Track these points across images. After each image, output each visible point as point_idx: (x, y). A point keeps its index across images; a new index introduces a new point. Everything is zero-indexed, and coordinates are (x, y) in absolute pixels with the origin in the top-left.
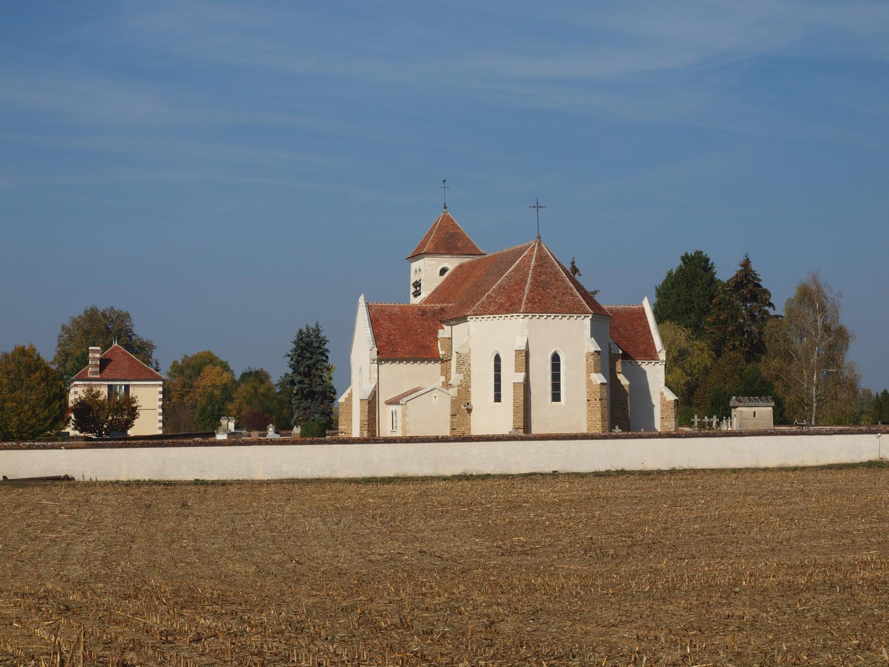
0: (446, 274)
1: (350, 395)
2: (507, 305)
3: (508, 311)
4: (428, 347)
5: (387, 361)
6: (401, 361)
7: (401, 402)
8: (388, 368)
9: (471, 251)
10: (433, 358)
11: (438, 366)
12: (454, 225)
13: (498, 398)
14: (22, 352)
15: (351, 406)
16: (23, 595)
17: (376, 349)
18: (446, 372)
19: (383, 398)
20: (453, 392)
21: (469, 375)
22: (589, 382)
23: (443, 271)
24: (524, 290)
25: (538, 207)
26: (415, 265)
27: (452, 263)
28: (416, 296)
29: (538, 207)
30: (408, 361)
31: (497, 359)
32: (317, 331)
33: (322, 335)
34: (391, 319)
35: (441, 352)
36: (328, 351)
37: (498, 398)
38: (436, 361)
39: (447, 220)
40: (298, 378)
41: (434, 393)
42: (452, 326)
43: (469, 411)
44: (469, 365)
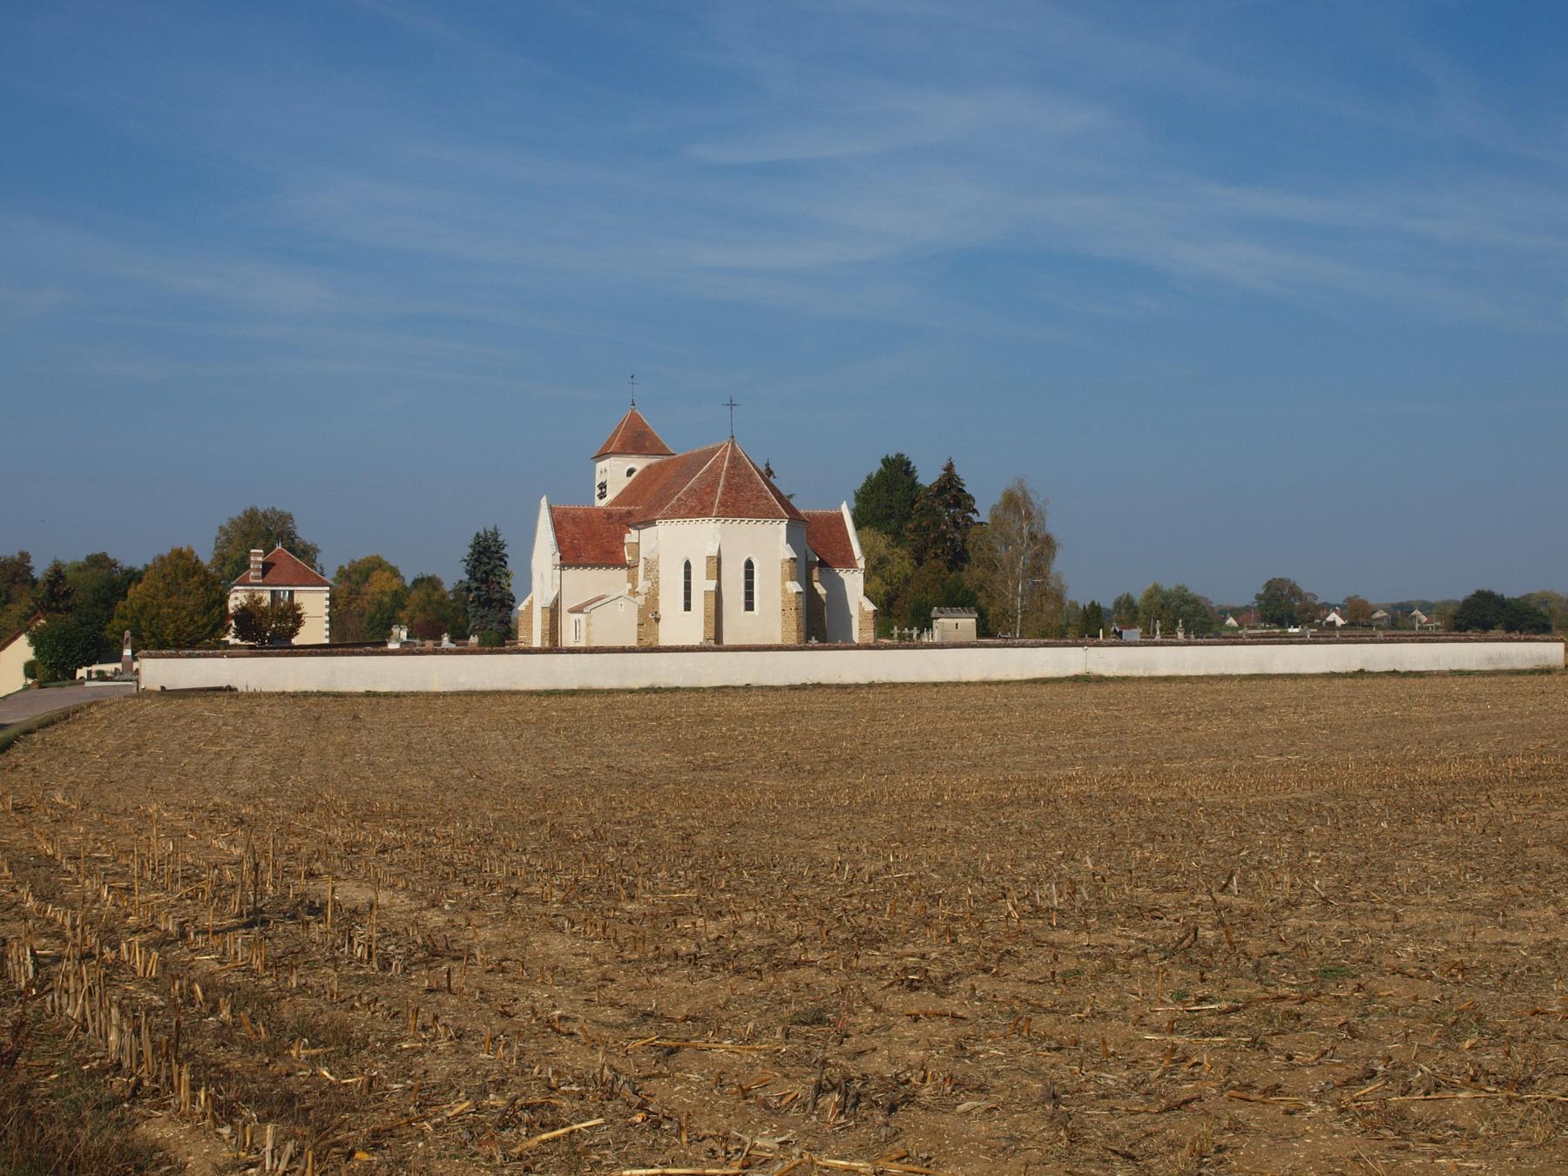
1: (531, 603)
2: (698, 508)
3: (699, 515)
5: (570, 567)
6: (585, 567)
8: (570, 574)
9: (659, 450)
10: (622, 564)
11: (624, 573)
13: (687, 607)
14: (179, 554)
16: (192, 809)
18: (633, 579)
19: (566, 605)
20: (640, 600)
22: (785, 591)
23: (630, 472)
25: (731, 405)
26: (600, 465)
27: (639, 463)
29: (731, 405)
30: (593, 567)
31: (688, 566)
32: (495, 534)
33: (500, 539)
35: (628, 558)
37: (687, 607)
39: (634, 418)
40: (475, 585)
41: (620, 602)
43: (657, 620)
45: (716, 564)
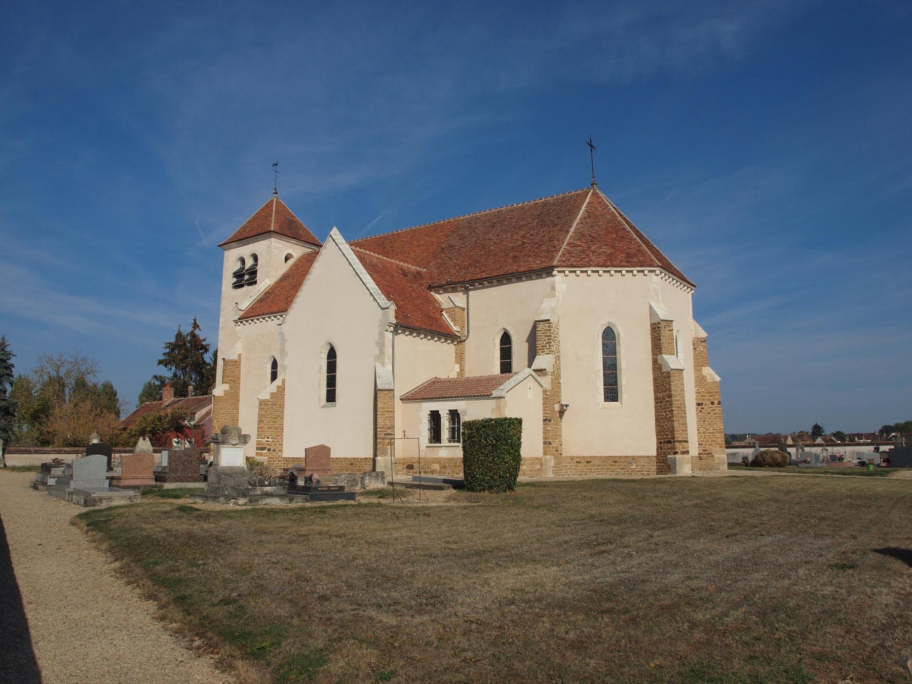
0: (291, 262)
4: (436, 319)
7: (495, 393)
8: (405, 341)
10: (447, 335)
11: (448, 349)
13: (612, 393)
15: (282, 407)
17: (393, 308)
18: (460, 358)
20: (546, 381)
28: (237, 286)
31: (609, 336)
33: (8, 349)
35: (455, 328)
36: (13, 365)
37: (612, 393)
42: (466, 291)
43: (562, 413)
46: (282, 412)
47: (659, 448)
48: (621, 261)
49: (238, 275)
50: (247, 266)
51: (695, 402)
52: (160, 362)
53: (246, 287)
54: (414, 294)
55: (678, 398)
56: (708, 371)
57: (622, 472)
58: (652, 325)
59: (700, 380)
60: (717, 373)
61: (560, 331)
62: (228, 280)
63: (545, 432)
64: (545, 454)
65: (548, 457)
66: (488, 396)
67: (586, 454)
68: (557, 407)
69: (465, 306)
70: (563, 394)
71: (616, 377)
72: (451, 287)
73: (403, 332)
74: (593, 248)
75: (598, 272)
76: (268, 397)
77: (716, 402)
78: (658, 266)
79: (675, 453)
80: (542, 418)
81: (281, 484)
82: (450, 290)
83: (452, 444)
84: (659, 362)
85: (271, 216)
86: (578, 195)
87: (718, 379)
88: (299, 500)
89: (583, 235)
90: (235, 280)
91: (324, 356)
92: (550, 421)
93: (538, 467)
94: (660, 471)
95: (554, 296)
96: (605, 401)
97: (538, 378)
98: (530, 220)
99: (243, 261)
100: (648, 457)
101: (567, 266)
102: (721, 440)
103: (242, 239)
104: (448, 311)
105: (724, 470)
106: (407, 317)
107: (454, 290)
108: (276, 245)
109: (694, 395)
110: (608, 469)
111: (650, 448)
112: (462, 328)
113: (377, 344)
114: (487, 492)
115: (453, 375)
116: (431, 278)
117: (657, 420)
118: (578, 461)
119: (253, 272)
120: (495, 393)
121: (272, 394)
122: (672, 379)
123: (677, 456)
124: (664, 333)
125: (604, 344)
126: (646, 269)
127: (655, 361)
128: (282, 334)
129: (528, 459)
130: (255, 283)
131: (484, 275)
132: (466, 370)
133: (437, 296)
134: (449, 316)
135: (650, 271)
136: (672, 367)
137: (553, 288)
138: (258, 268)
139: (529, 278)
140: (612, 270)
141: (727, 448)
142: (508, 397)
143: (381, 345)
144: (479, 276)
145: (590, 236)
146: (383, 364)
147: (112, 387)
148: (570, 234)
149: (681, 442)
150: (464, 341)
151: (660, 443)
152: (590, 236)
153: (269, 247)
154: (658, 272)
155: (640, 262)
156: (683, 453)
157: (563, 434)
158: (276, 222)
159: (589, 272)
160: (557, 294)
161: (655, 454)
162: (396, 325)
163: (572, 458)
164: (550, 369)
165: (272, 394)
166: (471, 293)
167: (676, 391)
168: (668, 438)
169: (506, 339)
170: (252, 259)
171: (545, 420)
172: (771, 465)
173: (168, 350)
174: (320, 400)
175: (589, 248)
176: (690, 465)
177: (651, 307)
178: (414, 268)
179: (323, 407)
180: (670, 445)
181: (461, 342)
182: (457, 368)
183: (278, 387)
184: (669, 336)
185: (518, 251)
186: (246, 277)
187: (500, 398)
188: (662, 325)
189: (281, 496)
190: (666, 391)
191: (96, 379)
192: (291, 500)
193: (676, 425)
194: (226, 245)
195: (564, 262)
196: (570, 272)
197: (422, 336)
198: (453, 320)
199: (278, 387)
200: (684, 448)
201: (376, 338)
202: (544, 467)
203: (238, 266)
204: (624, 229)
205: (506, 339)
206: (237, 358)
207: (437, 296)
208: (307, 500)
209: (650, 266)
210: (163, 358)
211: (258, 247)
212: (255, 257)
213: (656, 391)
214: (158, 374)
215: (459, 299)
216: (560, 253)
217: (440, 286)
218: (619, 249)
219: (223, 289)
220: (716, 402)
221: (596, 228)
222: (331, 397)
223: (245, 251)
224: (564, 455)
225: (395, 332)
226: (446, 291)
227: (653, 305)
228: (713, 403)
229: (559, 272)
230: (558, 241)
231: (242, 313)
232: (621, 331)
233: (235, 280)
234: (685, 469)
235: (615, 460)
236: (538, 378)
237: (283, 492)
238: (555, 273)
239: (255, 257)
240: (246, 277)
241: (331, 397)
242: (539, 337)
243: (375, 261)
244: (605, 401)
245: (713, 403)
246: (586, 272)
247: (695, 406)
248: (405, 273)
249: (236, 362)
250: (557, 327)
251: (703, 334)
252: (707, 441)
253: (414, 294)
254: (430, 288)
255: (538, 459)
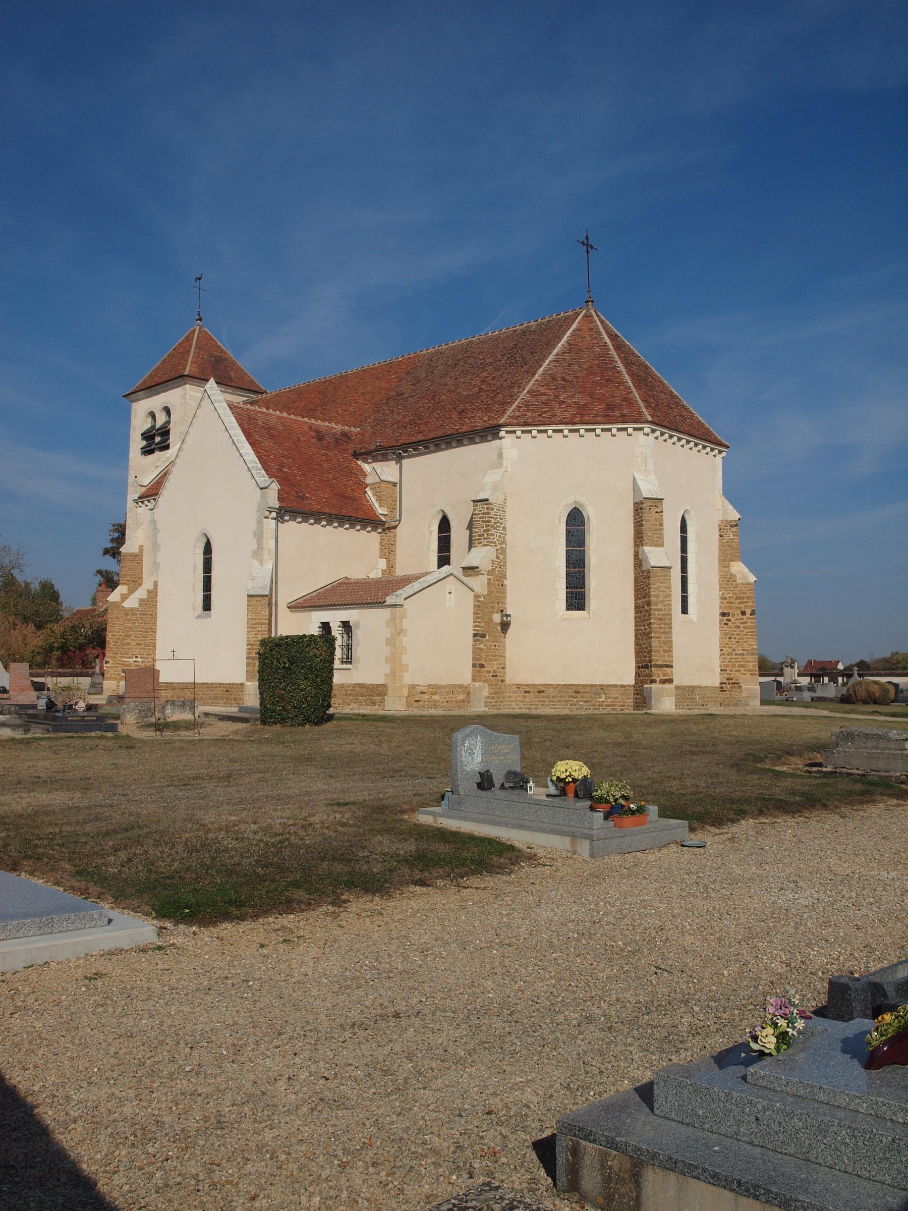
1: (153, 594)
4: (354, 500)
7: (390, 600)
8: (294, 529)
10: (370, 521)
11: (370, 539)
12: (218, 347)
13: (576, 598)
15: (154, 617)
17: (275, 487)
18: (388, 551)
19: (285, 597)
20: (479, 584)
21: (503, 551)
24: (622, 383)
25: (587, 245)
28: (147, 451)
29: (587, 245)
31: (576, 521)
34: (272, 437)
35: (381, 511)
37: (576, 598)
38: (375, 529)
42: (399, 459)
43: (505, 626)
44: (504, 529)
45: (644, 515)
46: (155, 624)
47: (638, 675)
48: (597, 416)
49: (148, 436)
50: (159, 424)
51: (718, 611)
52: (106, 552)
53: (157, 453)
54: (326, 465)
55: (660, 606)
56: (739, 569)
57: (586, 705)
58: (635, 504)
59: (727, 580)
60: (752, 570)
61: (507, 514)
62: (137, 443)
63: (476, 652)
64: (474, 680)
65: (477, 684)
66: (379, 604)
67: (538, 681)
68: (497, 618)
69: (398, 481)
70: (508, 600)
71: (584, 577)
72: (380, 454)
73: (293, 519)
74: (562, 398)
75: (561, 431)
76: (136, 605)
77: (748, 611)
78: (647, 422)
79: (653, 681)
80: (471, 633)
81: (17, 713)
82: (379, 458)
83: (345, 666)
84: (640, 556)
85: (189, 352)
86: (567, 318)
87: (752, 578)
88: (38, 730)
89: (554, 379)
90: (144, 443)
91: (201, 551)
92: (483, 636)
93: (461, 697)
94: (637, 706)
95: (500, 465)
96: (568, 609)
97: (465, 580)
98: (499, 356)
99: (153, 415)
100: (623, 686)
101: (518, 425)
102: (753, 665)
103: (152, 387)
104: (374, 486)
105: (755, 706)
106: (304, 498)
107: (385, 458)
108: (192, 393)
109: (718, 601)
110: (565, 701)
111: (625, 673)
112: (392, 509)
113: (255, 536)
114: (278, 726)
115: (376, 573)
116: (361, 441)
117: (636, 636)
118: (526, 690)
119: (165, 432)
120: (390, 600)
121: (141, 600)
122: (652, 580)
123: (653, 685)
124: (649, 517)
125: (568, 532)
126: (630, 426)
127: (636, 555)
128: (154, 522)
129: (444, 687)
130: (167, 447)
131: (420, 437)
132: (397, 566)
133: (366, 467)
134: (374, 495)
135: (635, 429)
136: (653, 564)
137: (500, 455)
138: (171, 426)
139: (472, 441)
140: (582, 428)
141: (761, 675)
142: (407, 604)
143: (259, 535)
144: (413, 439)
145: (563, 379)
146: (261, 562)
147: (52, 586)
148: (536, 377)
149: (661, 666)
150: (395, 527)
151: (639, 667)
152: (563, 379)
153: (184, 397)
154: (647, 430)
155: (623, 416)
156: (663, 682)
157: (508, 654)
158: (194, 362)
159: (550, 432)
160: (505, 463)
161: (633, 682)
162: (280, 509)
163: (518, 686)
164: (485, 566)
165: (141, 601)
166: (404, 462)
167: (657, 597)
168: (648, 663)
169: (445, 525)
170: (164, 414)
171: (475, 635)
172: (865, 702)
173: (116, 535)
174: (194, 608)
175: (557, 397)
176: (673, 699)
177: (634, 480)
178: (338, 428)
179: (199, 617)
180: (647, 671)
181: (389, 528)
182: (382, 564)
183: (149, 591)
184: (656, 520)
185: (451, 403)
186: (158, 439)
187: (395, 606)
188: (646, 505)
189: (14, 727)
190: (644, 597)
191: (30, 575)
192: (27, 731)
193: (655, 643)
194: (132, 395)
195: (516, 418)
196: (523, 432)
197: (324, 523)
198: (379, 499)
199: (149, 591)
200: (665, 675)
201: (253, 526)
202: (472, 698)
203: (148, 425)
204: (615, 368)
205: (445, 525)
206: (137, 551)
207: (366, 467)
208: (48, 731)
209: (635, 422)
210: (109, 545)
211: (172, 397)
212: (167, 411)
213: (637, 598)
214: (103, 568)
215: (387, 470)
216: (515, 405)
217: (368, 453)
218: (602, 396)
219: (131, 455)
220: (748, 611)
221: (576, 367)
222: (207, 605)
223: (155, 402)
224: (508, 682)
225: (280, 518)
226: (375, 460)
227: (637, 476)
228: (743, 613)
229: (507, 432)
230: (519, 387)
231: (144, 489)
232: (591, 514)
233: (144, 443)
234: (665, 703)
235: (577, 690)
236: (465, 580)
237: (19, 722)
238: (502, 434)
239: (167, 411)
240: (158, 439)
241: (207, 606)
242: (485, 520)
243: (273, 421)
244: (568, 609)
245: (743, 613)
246: (546, 431)
247: (718, 617)
248: (320, 436)
249: (136, 555)
250: (502, 509)
251: (734, 515)
252: (733, 666)
253: (326, 465)
254: (356, 455)
255: (461, 686)
